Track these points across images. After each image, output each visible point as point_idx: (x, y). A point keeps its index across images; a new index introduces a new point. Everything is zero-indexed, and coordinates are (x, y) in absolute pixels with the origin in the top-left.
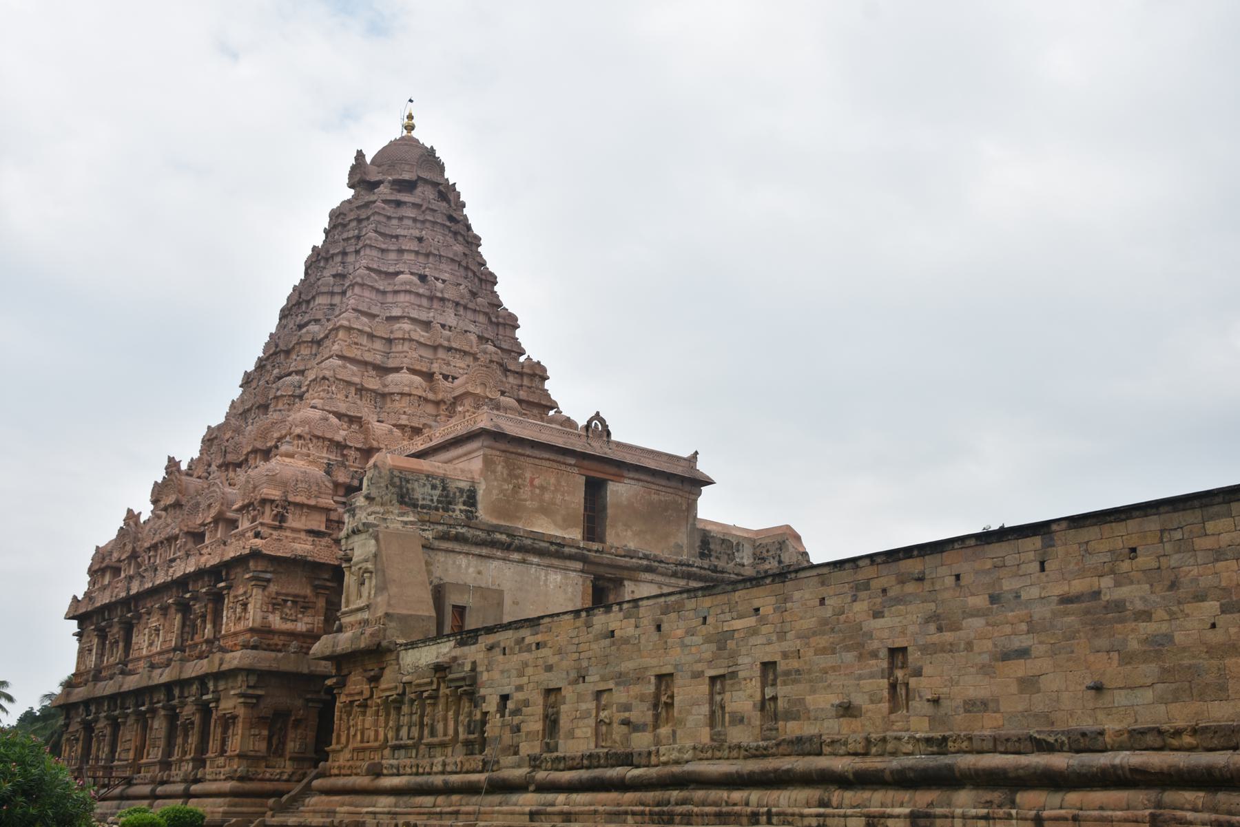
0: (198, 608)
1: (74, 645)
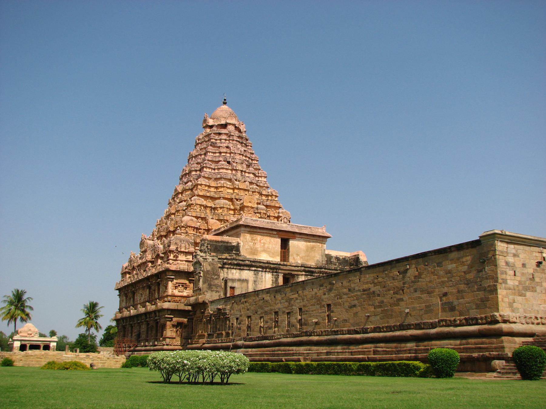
0: (153, 287)
1: (118, 299)
